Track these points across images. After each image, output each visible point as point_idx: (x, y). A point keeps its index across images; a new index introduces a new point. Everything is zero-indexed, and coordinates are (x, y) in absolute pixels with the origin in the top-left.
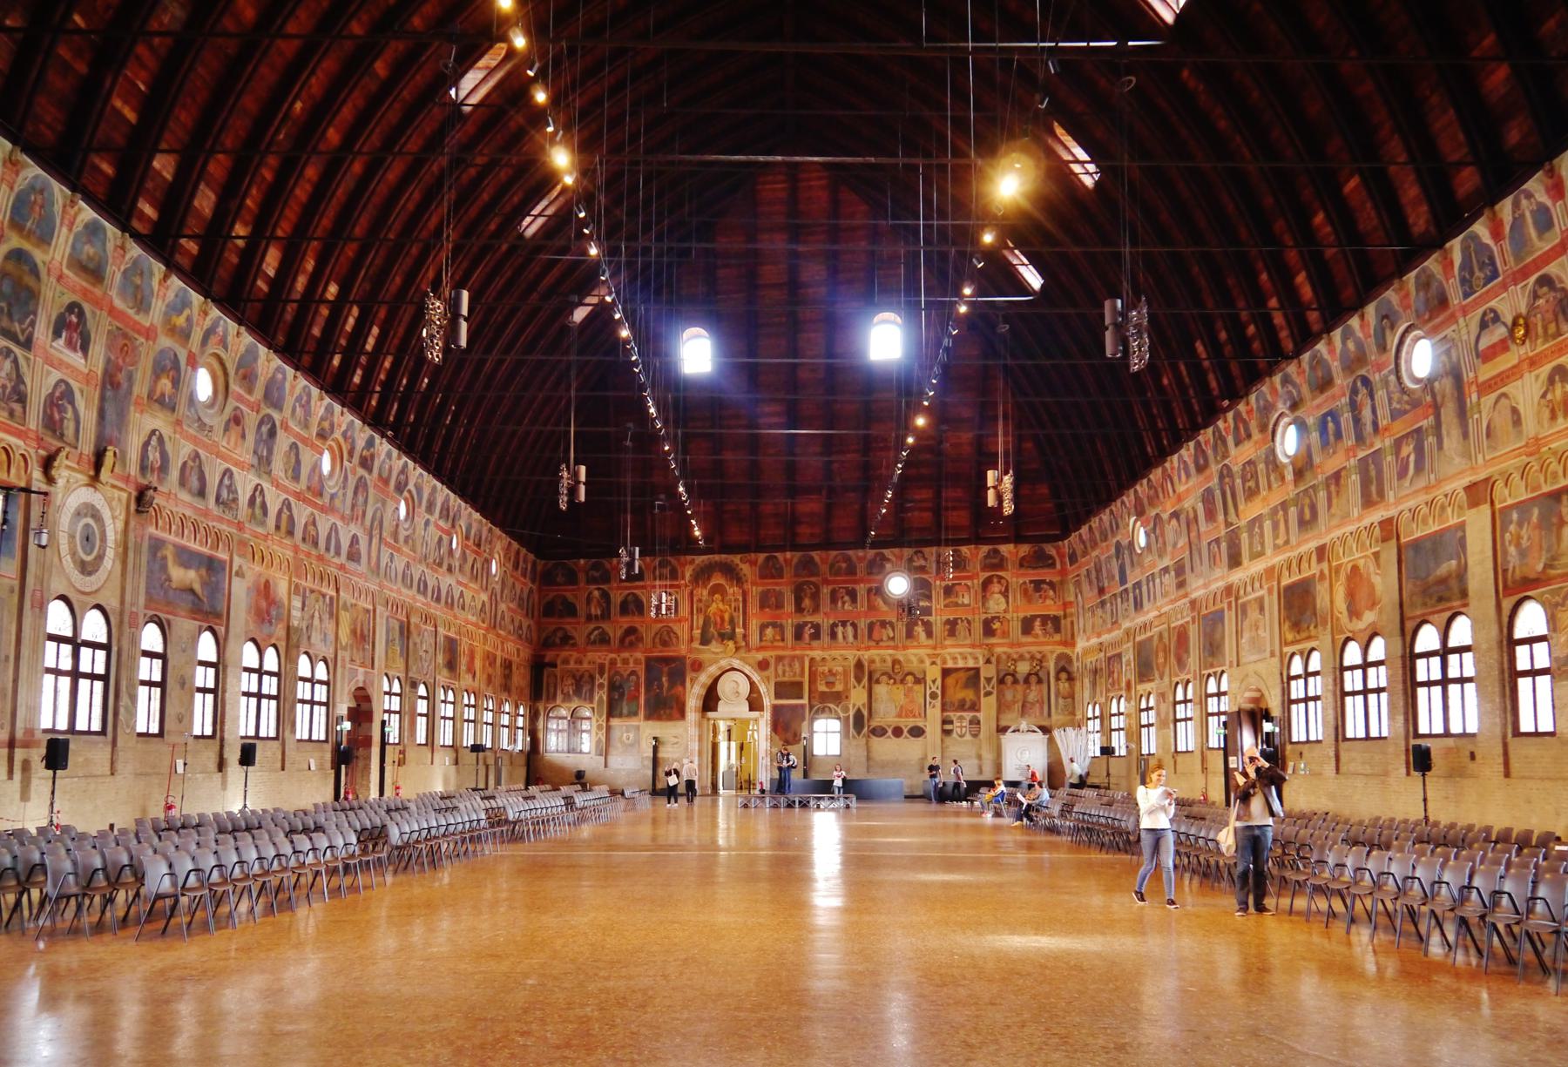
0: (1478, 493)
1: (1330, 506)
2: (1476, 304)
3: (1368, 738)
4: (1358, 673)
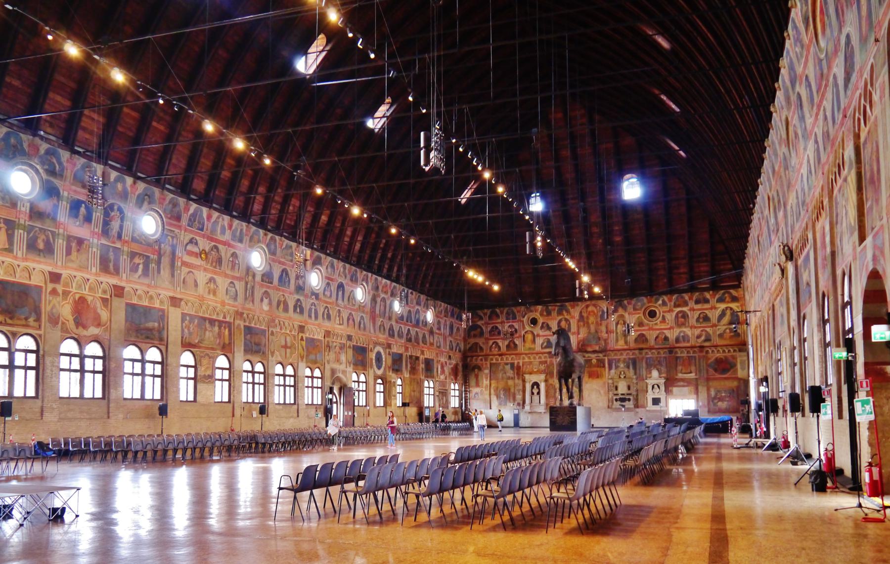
0: (175, 302)
1: (69, 253)
2: (191, 232)
3: (285, 403)
4: (315, 385)
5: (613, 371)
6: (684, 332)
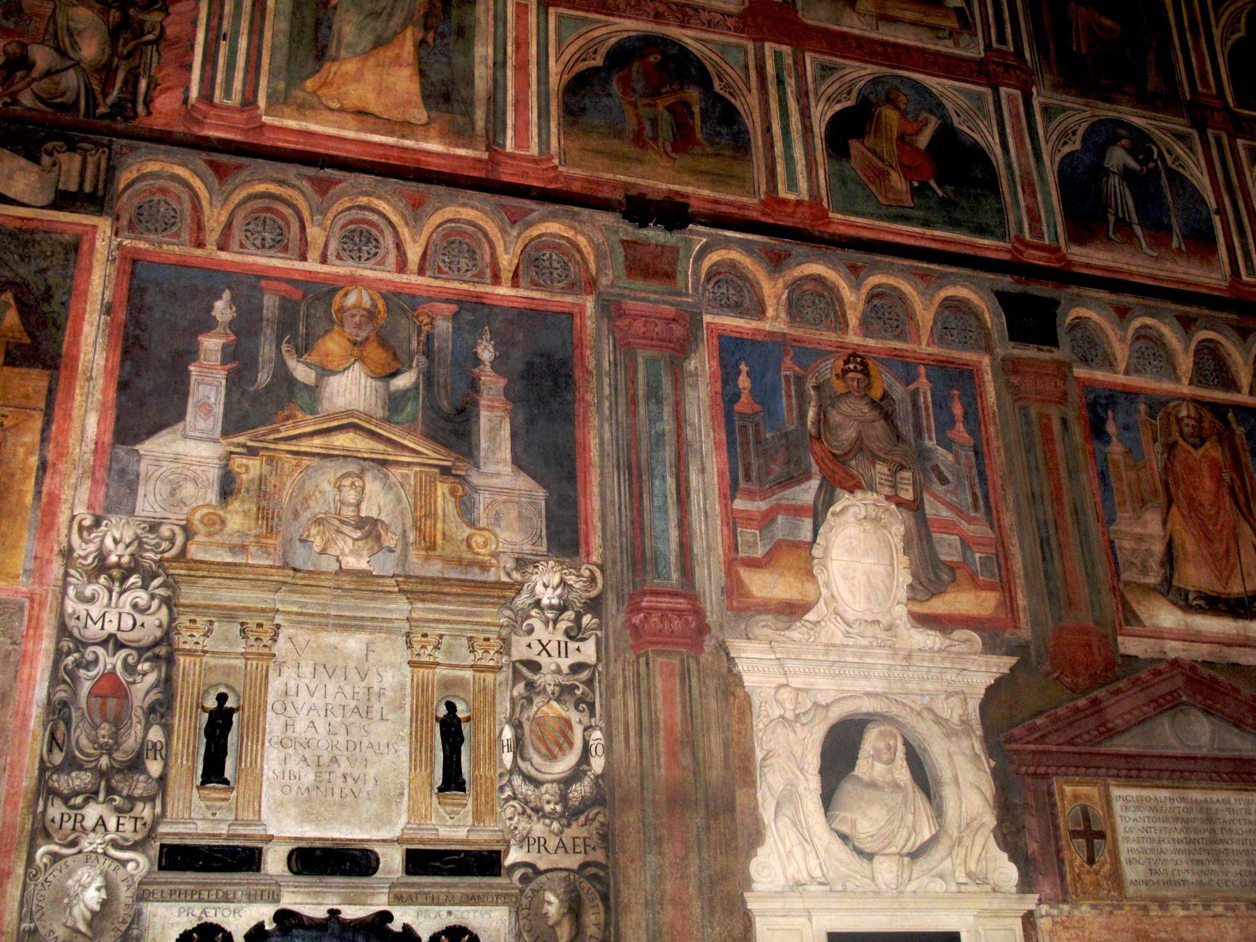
5: (187, 452)
6: (1140, 143)
